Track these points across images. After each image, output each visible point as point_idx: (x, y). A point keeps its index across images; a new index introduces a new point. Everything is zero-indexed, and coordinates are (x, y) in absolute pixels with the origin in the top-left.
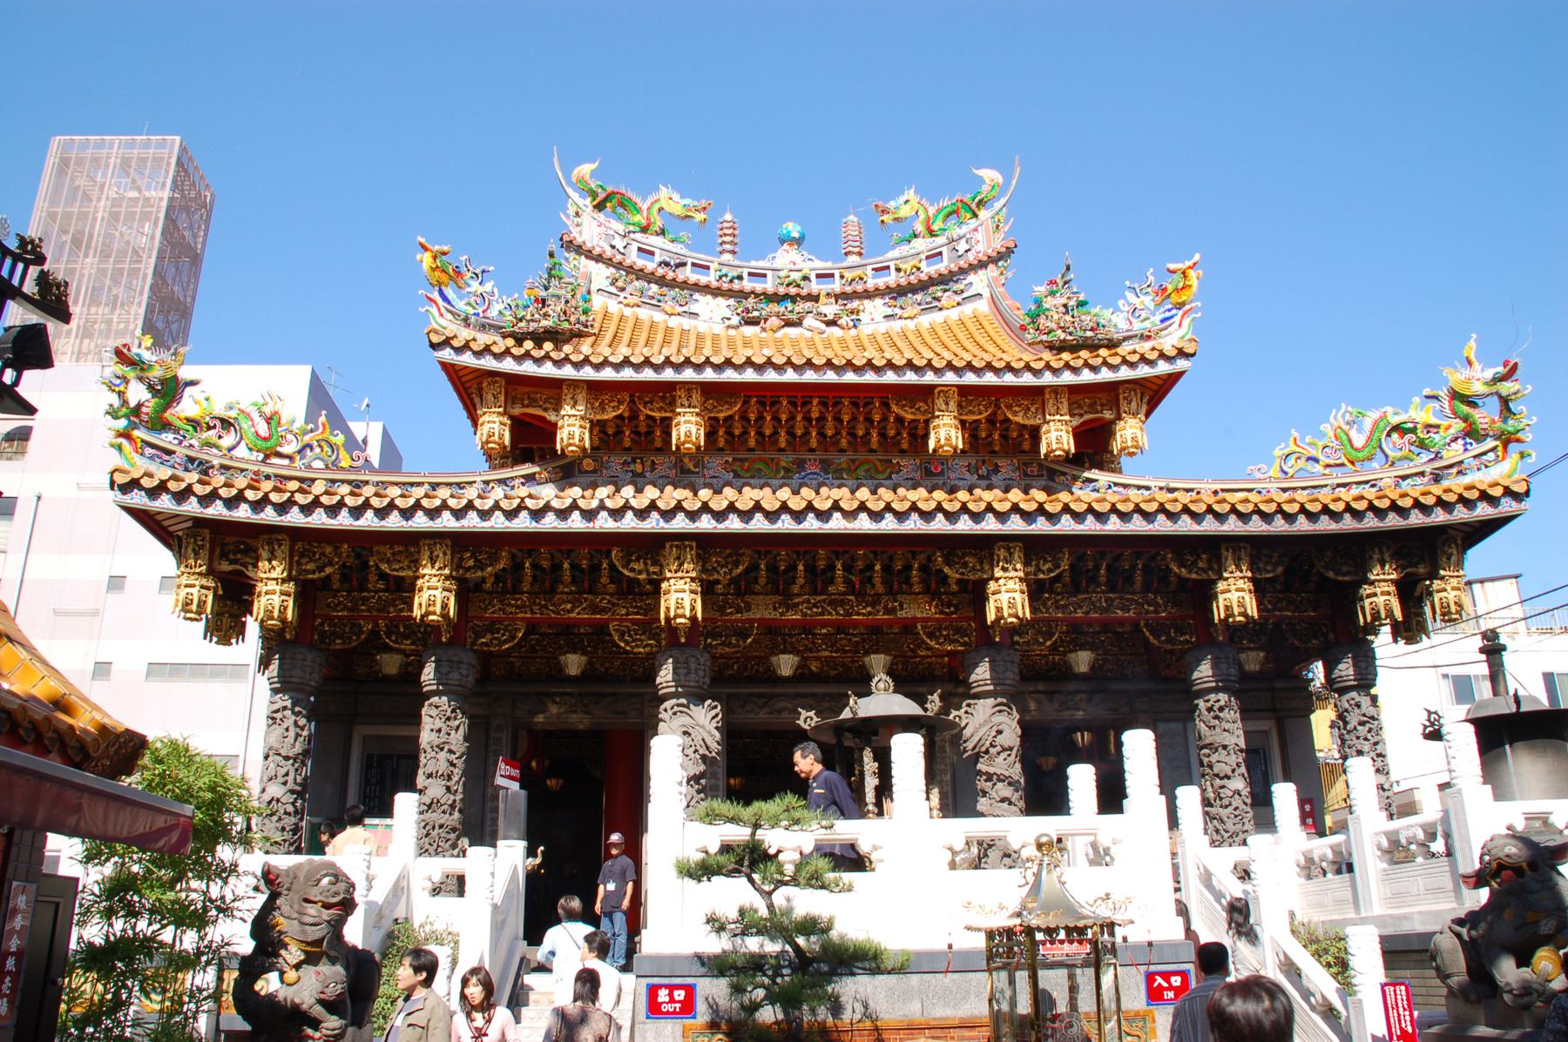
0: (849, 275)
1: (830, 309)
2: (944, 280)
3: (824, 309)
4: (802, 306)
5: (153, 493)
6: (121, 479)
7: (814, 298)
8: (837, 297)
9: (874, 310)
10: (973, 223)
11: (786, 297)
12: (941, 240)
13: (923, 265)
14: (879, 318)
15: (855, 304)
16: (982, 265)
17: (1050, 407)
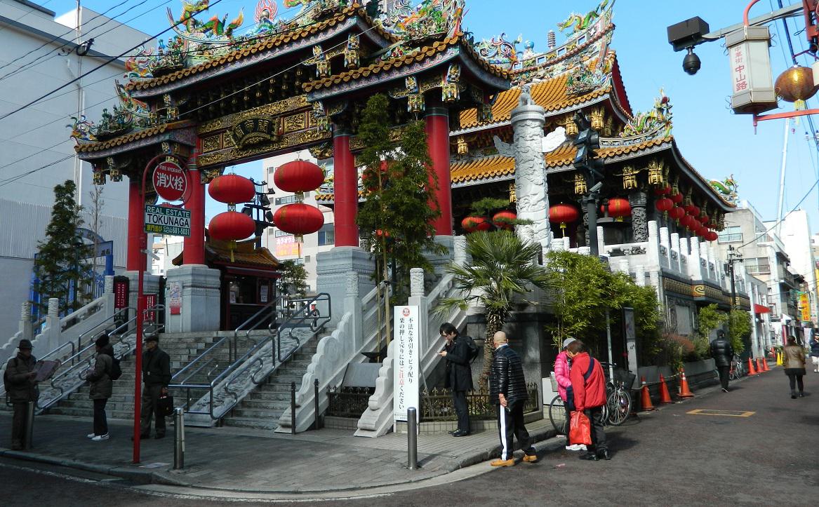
0: (549, 57)
1: (541, 73)
2: (584, 48)
3: (539, 73)
4: (532, 74)
5: (324, 200)
6: (317, 198)
7: (535, 69)
8: (544, 67)
9: (560, 66)
10: (597, 19)
11: (525, 72)
12: (584, 31)
13: (577, 45)
14: (560, 71)
15: (550, 68)
16: (599, 37)
17: (567, 119)
